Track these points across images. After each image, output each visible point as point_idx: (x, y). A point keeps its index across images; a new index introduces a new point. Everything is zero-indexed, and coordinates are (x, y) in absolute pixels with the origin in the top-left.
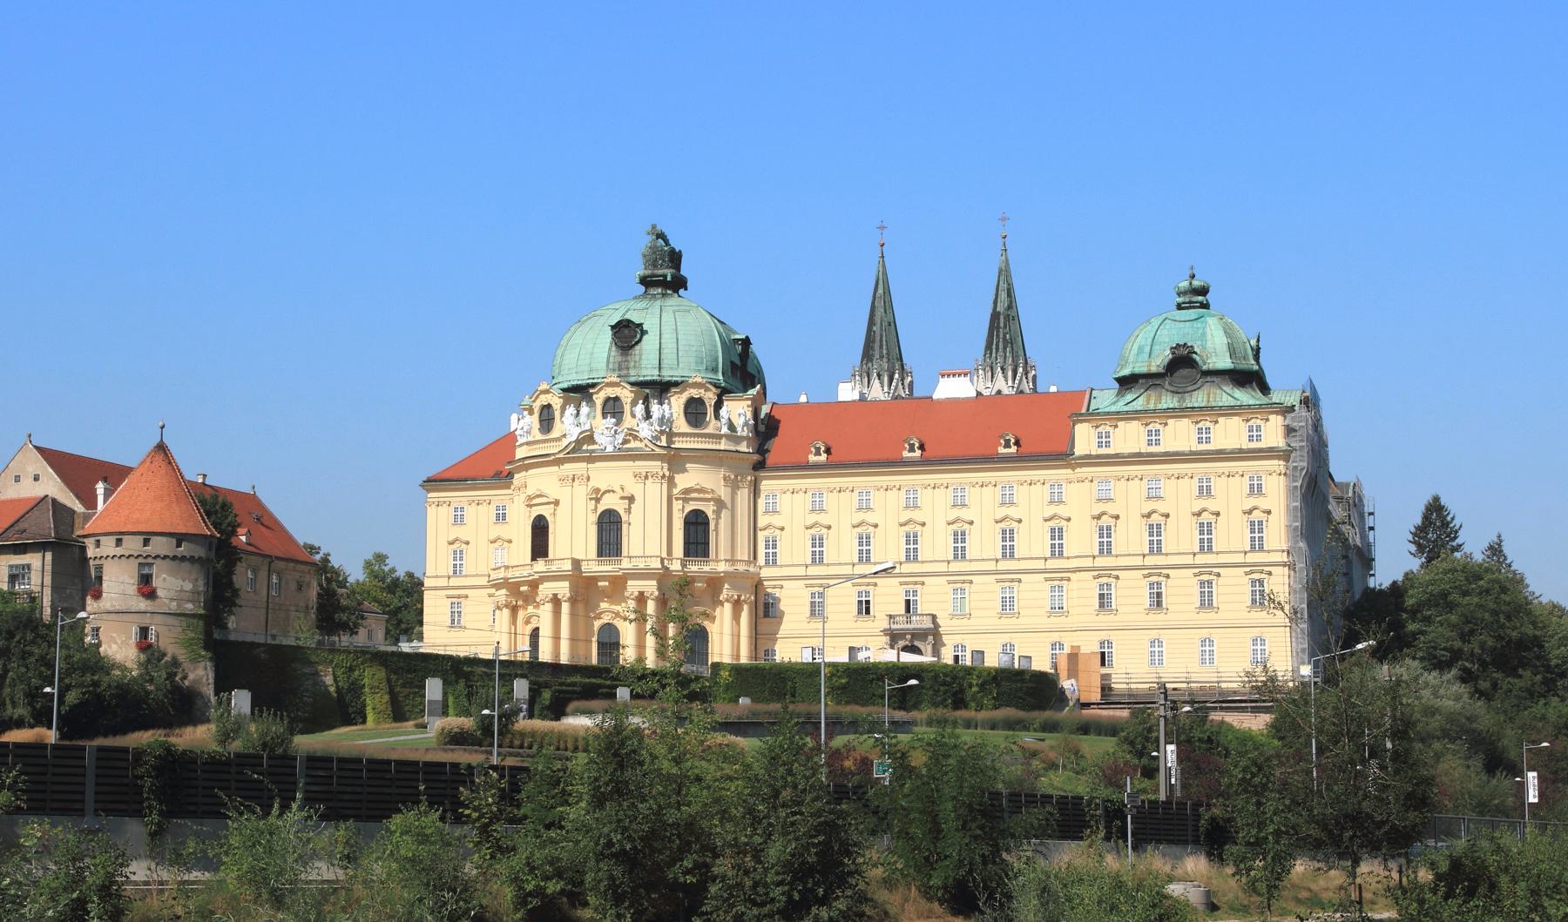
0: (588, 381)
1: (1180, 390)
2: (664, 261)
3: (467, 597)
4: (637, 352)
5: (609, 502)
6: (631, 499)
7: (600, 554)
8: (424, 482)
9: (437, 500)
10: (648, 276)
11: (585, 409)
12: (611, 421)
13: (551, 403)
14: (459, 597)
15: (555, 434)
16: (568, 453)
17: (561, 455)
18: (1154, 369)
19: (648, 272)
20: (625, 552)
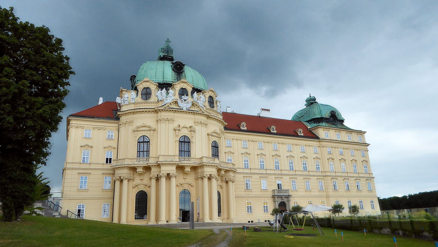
0: (164, 82)
1: (334, 124)
2: (171, 52)
3: (90, 174)
4: (184, 75)
5: (185, 132)
6: (194, 131)
7: (180, 155)
8: (69, 115)
9: (76, 125)
10: (166, 56)
11: (171, 91)
12: (184, 97)
13: (150, 87)
14: (86, 174)
15: (153, 98)
16: (165, 108)
17: (162, 108)
18: (327, 117)
19: (166, 54)
20: (192, 156)
